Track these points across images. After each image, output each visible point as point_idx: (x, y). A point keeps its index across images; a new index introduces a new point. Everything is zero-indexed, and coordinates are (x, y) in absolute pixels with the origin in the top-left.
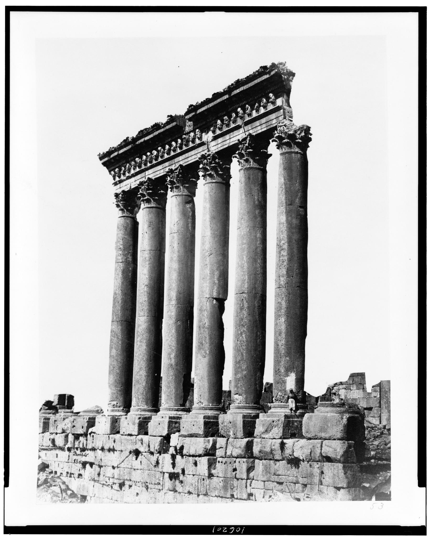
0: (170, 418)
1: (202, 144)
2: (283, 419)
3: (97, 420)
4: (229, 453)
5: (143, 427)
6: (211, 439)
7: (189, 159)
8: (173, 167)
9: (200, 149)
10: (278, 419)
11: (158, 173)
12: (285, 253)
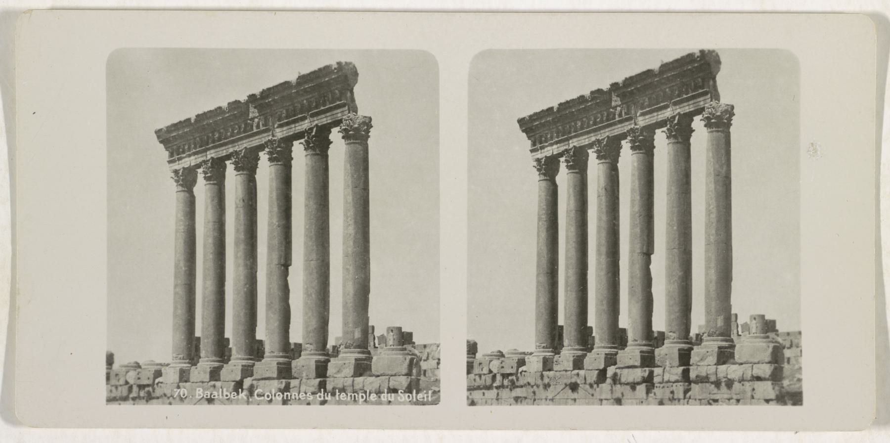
5: (578, 363)
6: (647, 369)
12: (713, 216)
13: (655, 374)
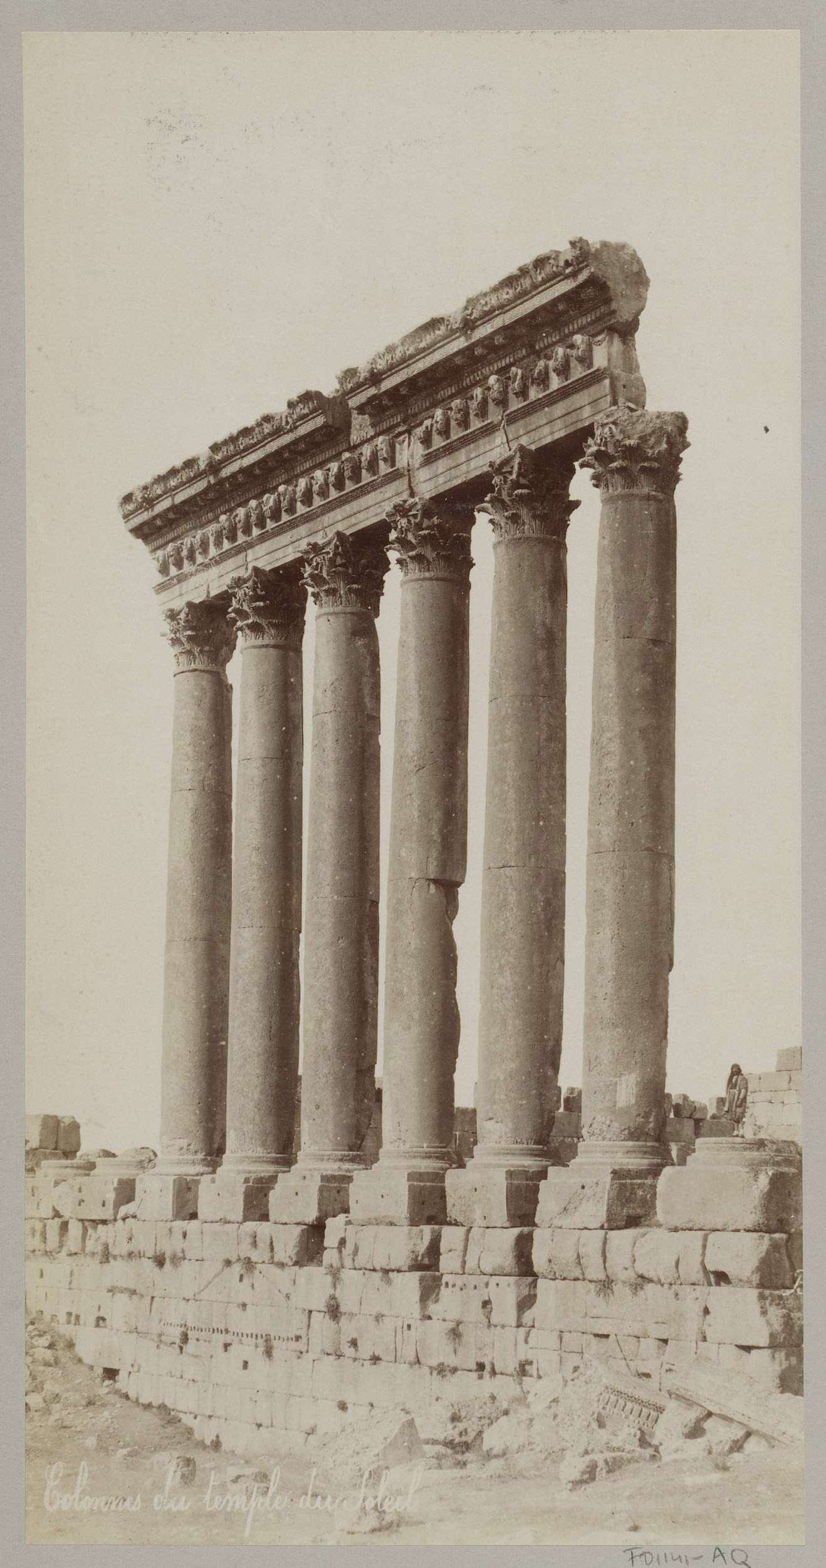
0: (324, 1178)
1: (395, 476)
2: (608, 1178)
3: (138, 1187)
4: (471, 1264)
5: (256, 1201)
6: (427, 1230)
7: (361, 516)
8: (320, 540)
9: (390, 490)
10: (595, 1180)
11: (280, 554)
13: (443, 1247)
